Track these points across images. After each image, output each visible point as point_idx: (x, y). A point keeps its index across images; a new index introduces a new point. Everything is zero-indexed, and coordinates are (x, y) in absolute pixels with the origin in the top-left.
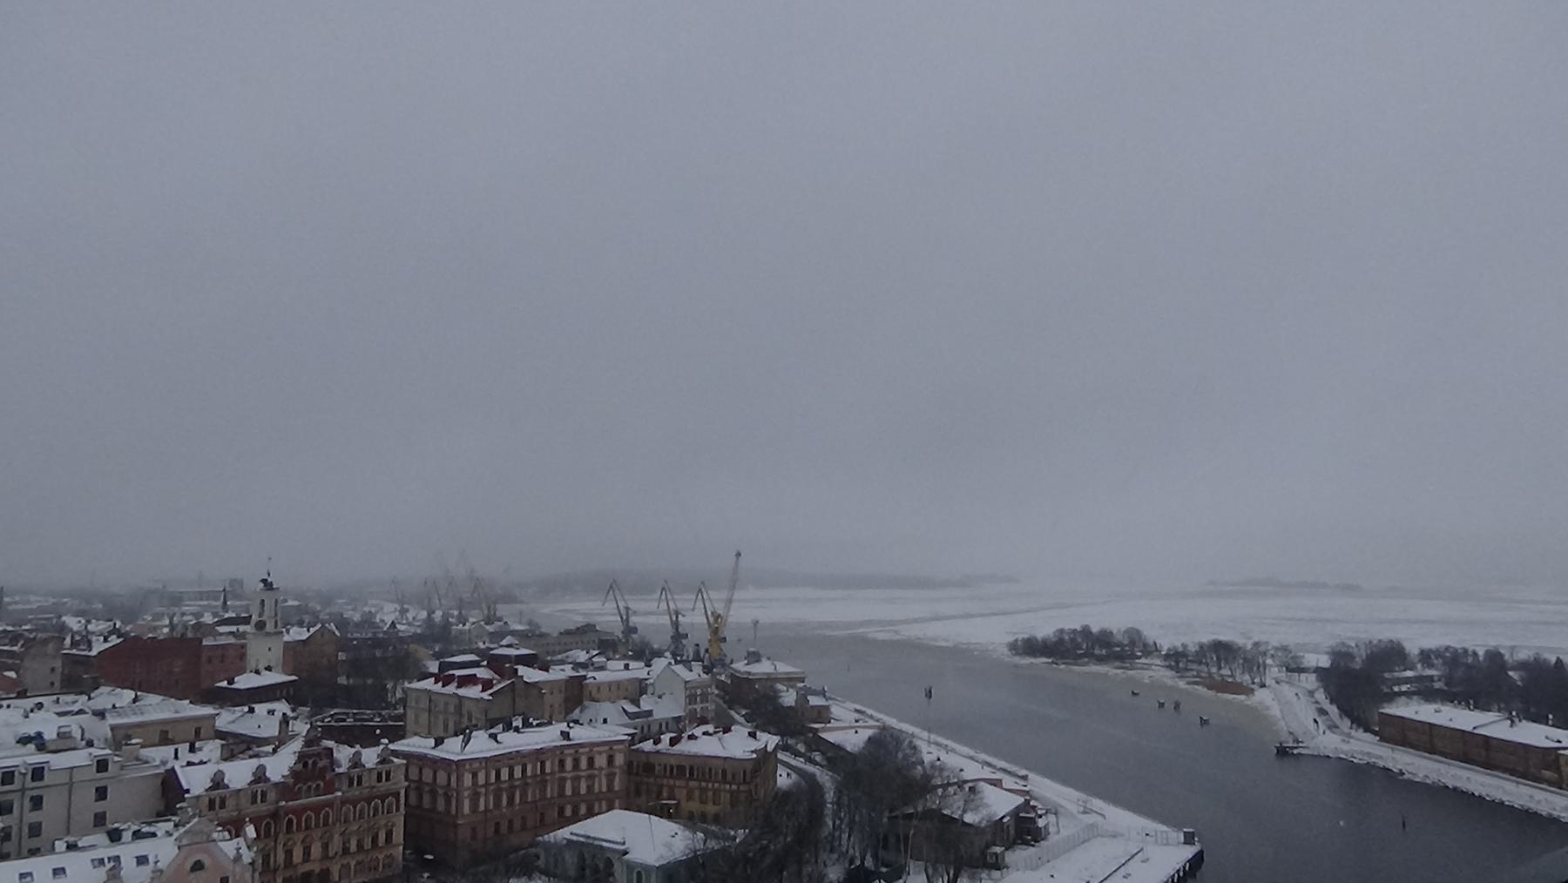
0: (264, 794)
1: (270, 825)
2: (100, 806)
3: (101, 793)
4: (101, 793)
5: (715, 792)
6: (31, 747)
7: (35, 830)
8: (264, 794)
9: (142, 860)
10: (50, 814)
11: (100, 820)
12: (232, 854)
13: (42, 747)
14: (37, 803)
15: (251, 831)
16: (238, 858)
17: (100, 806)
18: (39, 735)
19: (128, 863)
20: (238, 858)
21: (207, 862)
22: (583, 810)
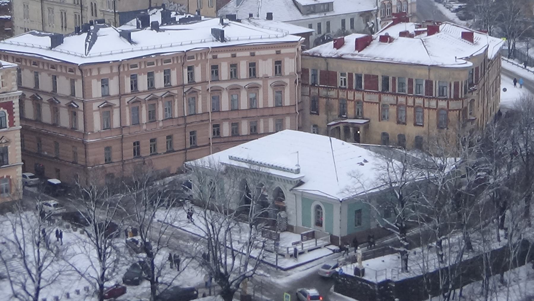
5: (359, 103)
22: (245, 129)
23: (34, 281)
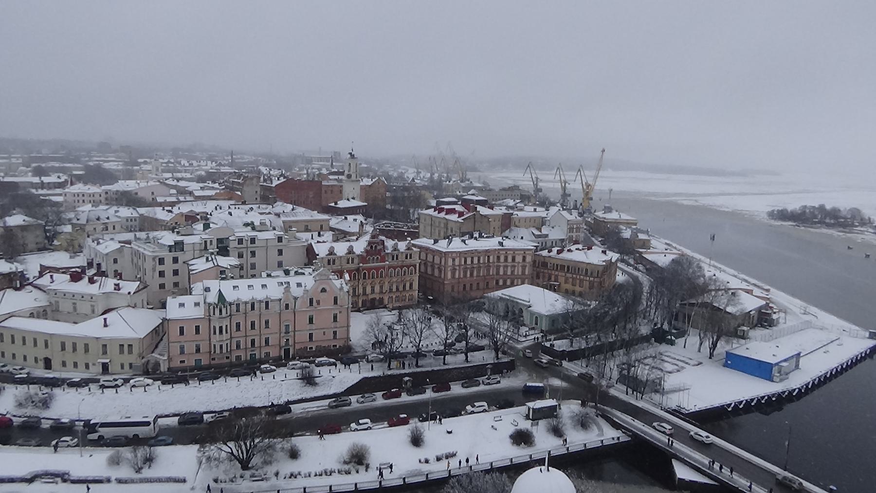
0: (353, 259)
1: (355, 274)
2: (280, 258)
3: (280, 252)
4: (280, 252)
5: (557, 276)
6: (249, 228)
7: (253, 266)
8: (353, 259)
9: (299, 285)
10: (259, 260)
11: (280, 264)
12: (339, 286)
13: (254, 229)
14: (253, 254)
15: (347, 276)
16: (341, 289)
17: (280, 258)
18: (252, 223)
19: (293, 286)
20: (341, 289)
21: (328, 290)
22: (508, 283)
23: (330, 364)
